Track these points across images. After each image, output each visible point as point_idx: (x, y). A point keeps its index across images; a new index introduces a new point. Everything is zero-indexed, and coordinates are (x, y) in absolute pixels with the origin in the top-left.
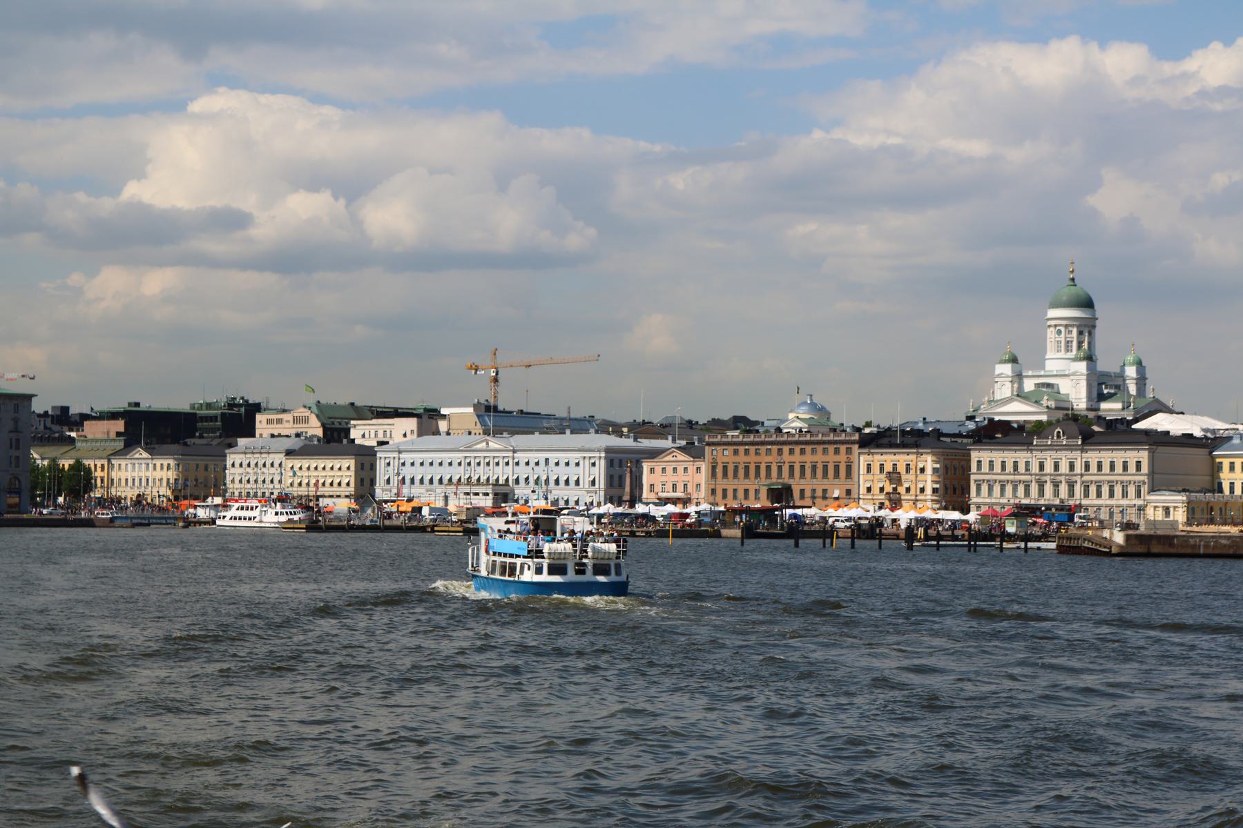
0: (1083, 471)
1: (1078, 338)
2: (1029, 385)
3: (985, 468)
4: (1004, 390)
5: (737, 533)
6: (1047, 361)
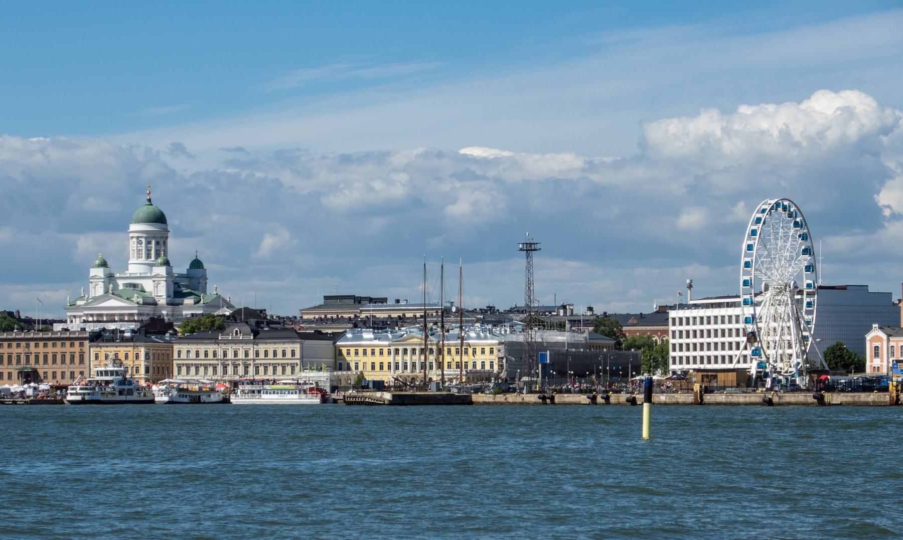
1: (155, 245)
4: (98, 290)
6: (129, 266)
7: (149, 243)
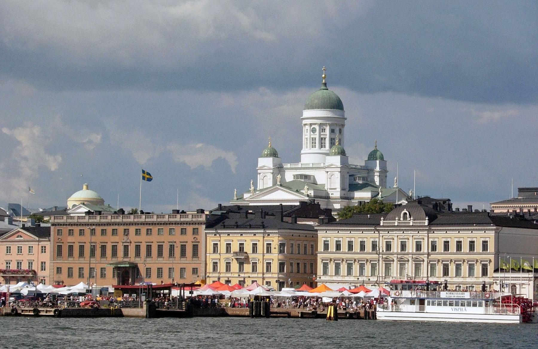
0: (430, 251)
1: (330, 134)
2: (289, 176)
3: (332, 247)
5: (142, 311)
6: (302, 155)
7: (324, 130)
